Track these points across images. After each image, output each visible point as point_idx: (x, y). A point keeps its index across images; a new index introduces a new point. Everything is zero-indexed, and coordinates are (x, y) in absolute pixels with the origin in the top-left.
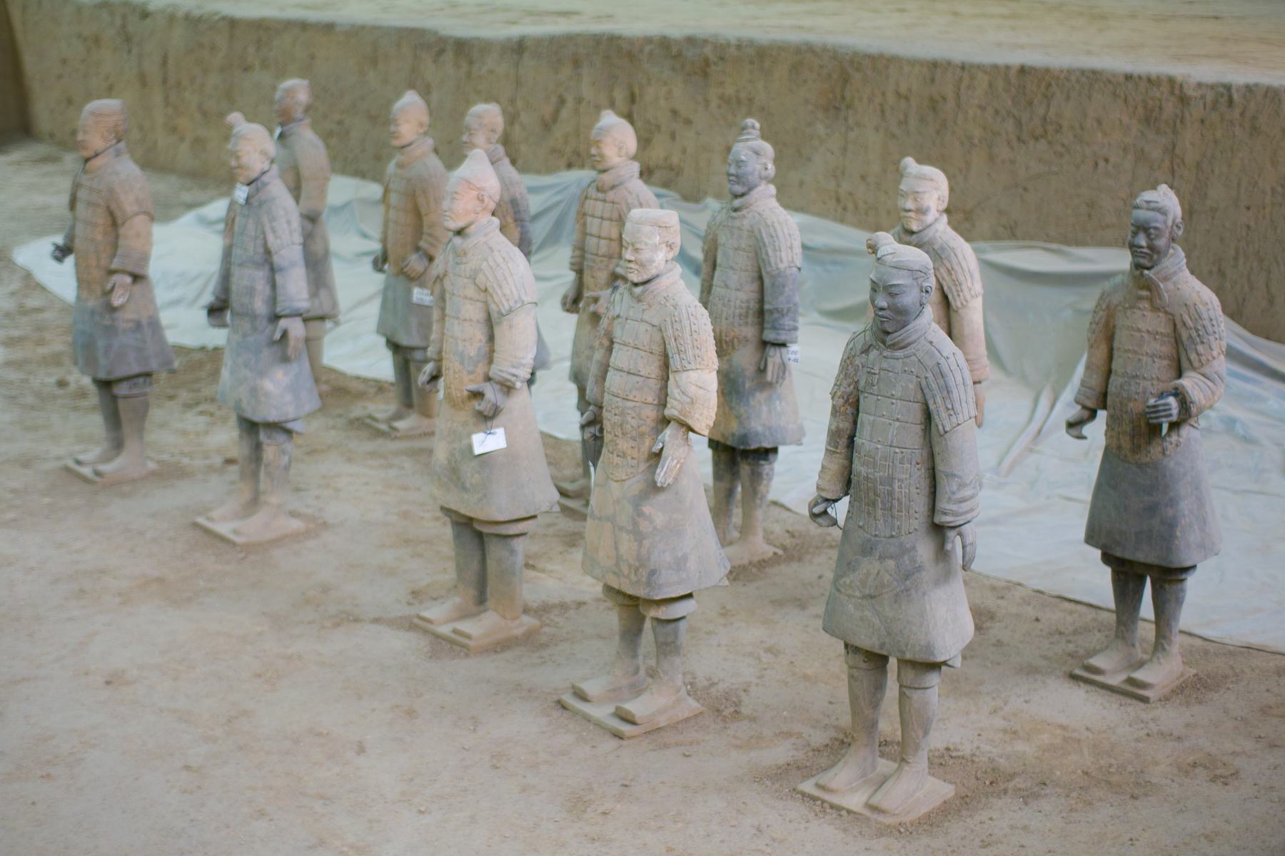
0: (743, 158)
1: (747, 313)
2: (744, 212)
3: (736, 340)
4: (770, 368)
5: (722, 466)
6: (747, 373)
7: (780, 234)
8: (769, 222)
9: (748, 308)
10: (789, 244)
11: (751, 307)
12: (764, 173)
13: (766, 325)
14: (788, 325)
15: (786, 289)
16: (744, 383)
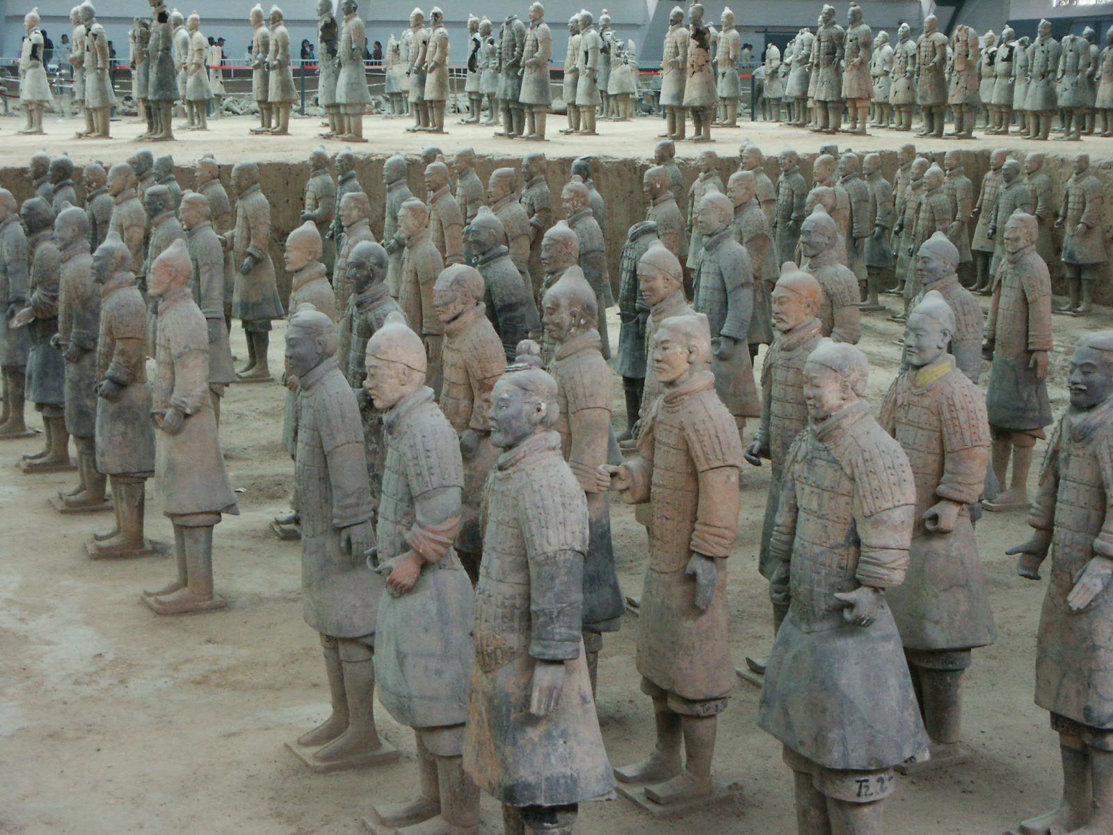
0: (505, 396)
1: (513, 614)
2: (510, 471)
3: (499, 652)
4: (536, 695)
5: (512, 823)
6: (513, 700)
7: (549, 502)
8: (536, 487)
9: (514, 606)
10: (560, 518)
11: (518, 605)
12: (536, 417)
13: (533, 634)
14: (560, 633)
15: (557, 581)
16: (509, 710)
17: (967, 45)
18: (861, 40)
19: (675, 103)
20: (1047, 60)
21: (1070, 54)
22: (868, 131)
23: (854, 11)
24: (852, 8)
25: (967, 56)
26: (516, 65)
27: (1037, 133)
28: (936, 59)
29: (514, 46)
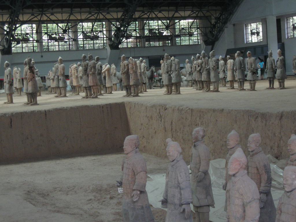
20: (168, 67)
21: (174, 65)
22: (98, 97)
23: (89, 56)
24: (89, 55)
28: (126, 69)
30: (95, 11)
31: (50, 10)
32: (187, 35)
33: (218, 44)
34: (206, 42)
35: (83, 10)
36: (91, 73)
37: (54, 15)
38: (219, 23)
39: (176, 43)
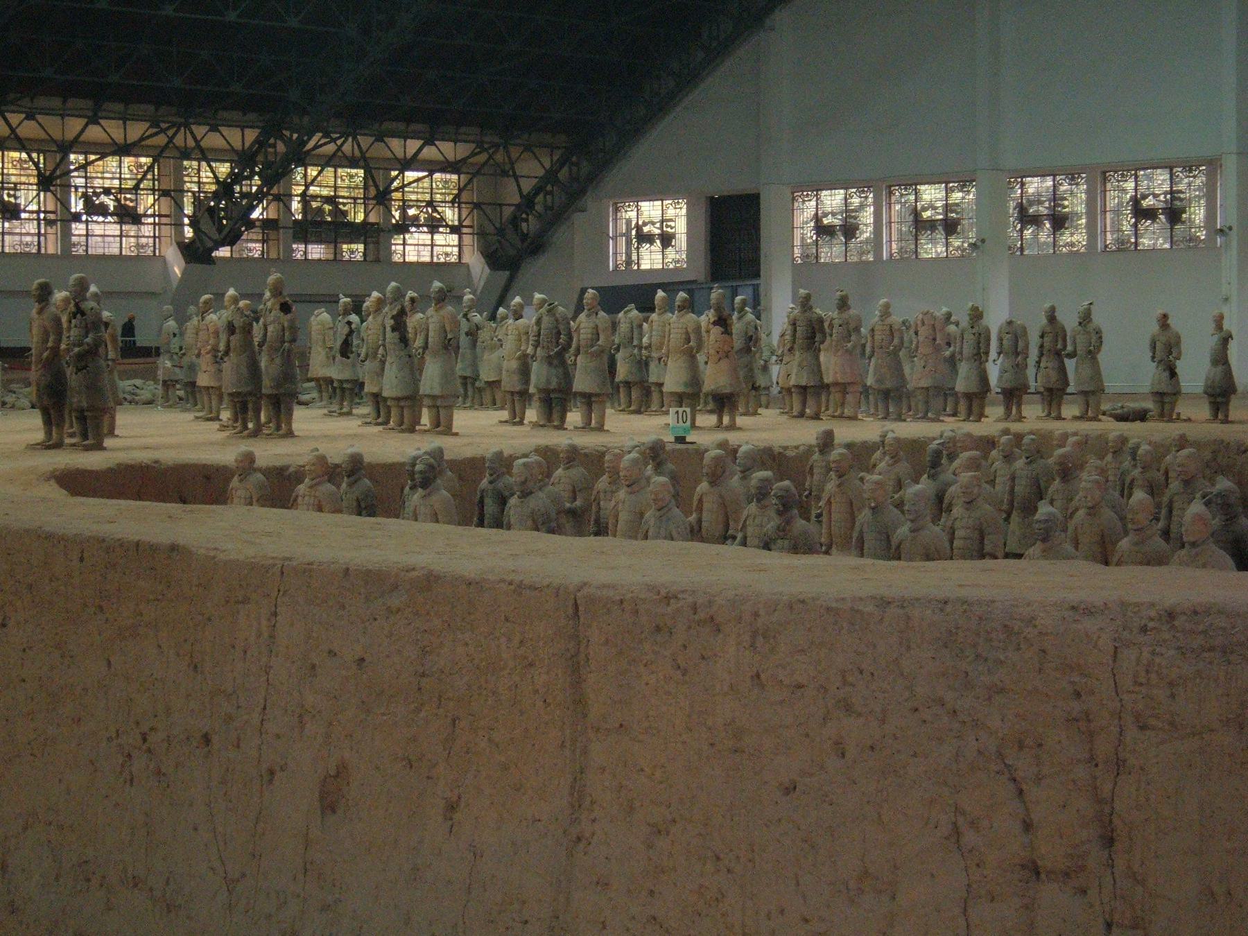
17: (934, 329)
18: (852, 326)
19: (689, 390)
25: (934, 339)
26: (561, 355)
27: (969, 414)
29: (559, 333)
30: (175, 119)
31: (26, 102)
32: (422, 226)
33: (532, 269)
34: (493, 258)
35: (135, 108)
36: (849, 345)
37: (99, 124)
38: (551, 193)
39: (390, 253)
